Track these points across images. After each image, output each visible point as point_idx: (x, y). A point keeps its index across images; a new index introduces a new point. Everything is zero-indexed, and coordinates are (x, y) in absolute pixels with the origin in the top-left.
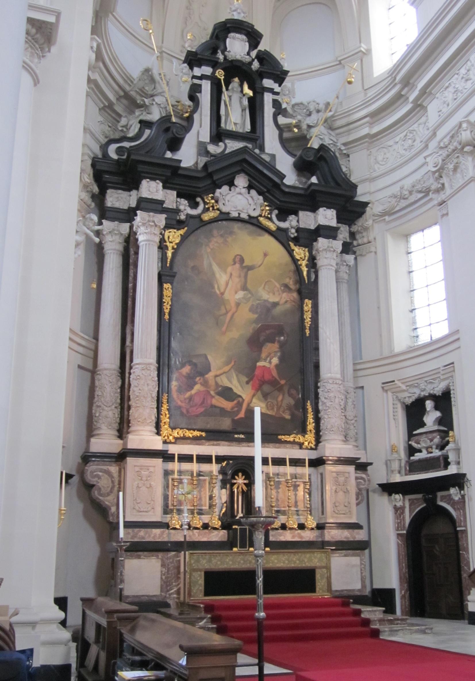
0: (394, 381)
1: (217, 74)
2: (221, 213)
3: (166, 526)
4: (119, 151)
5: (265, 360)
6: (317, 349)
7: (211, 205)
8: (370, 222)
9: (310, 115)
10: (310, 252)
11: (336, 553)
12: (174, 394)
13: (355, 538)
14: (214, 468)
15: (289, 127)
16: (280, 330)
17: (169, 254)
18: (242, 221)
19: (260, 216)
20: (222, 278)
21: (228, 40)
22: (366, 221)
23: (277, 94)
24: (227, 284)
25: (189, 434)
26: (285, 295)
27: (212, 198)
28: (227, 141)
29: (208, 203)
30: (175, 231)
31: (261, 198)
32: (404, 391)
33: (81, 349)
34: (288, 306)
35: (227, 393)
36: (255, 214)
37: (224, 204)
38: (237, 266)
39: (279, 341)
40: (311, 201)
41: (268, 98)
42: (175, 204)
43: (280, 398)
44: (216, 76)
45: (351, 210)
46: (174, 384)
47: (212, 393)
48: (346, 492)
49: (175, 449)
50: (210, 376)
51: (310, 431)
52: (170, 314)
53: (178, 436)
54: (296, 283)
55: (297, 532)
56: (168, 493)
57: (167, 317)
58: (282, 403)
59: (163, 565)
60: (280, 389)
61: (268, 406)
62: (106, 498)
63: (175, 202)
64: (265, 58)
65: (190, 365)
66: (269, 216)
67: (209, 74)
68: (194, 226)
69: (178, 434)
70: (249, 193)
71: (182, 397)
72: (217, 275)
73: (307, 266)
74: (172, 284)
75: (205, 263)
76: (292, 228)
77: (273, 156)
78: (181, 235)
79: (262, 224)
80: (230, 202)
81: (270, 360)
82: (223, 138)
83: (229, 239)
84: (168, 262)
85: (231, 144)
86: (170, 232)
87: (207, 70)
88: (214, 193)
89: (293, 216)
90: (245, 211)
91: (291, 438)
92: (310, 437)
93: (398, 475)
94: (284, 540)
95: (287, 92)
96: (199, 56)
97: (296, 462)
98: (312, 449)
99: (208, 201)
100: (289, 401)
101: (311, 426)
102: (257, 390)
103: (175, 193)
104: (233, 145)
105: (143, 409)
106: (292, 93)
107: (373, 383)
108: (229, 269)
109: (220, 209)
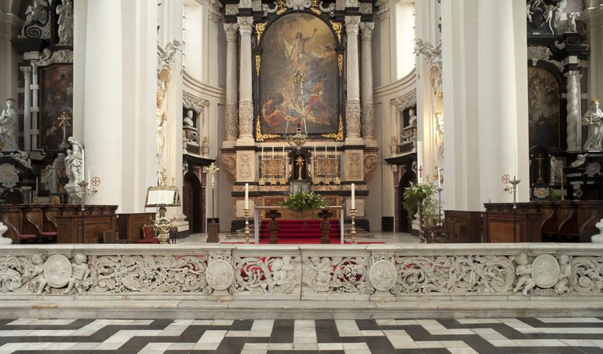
2: (288, 9)
3: (257, 184)
5: (315, 93)
12: (264, 115)
14: (284, 154)
17: (259, 38)
18: (301, 11)
19: (311, 7)
20: (289, 48)
25: (271, 136)
33: (219, 96)
34: (330, 59)
35: (293, 113)
36: (307, 6)
46: (264, 110)
49: (263, 145)
50: (283, 104)
54: (334, 45)
57: (258, 74)
60: (324, 109)
68: (272, 20)
72: (287, 47)
73: (341, 34)
74: (261, 55)
83: (293, 24)
91: (329, 136)
92: (341, 135)
98: (341, 141)
101: (341, 129)
102: (310, 110)
105: (246, 125)
107: (385, 100)
108: (294, 42)
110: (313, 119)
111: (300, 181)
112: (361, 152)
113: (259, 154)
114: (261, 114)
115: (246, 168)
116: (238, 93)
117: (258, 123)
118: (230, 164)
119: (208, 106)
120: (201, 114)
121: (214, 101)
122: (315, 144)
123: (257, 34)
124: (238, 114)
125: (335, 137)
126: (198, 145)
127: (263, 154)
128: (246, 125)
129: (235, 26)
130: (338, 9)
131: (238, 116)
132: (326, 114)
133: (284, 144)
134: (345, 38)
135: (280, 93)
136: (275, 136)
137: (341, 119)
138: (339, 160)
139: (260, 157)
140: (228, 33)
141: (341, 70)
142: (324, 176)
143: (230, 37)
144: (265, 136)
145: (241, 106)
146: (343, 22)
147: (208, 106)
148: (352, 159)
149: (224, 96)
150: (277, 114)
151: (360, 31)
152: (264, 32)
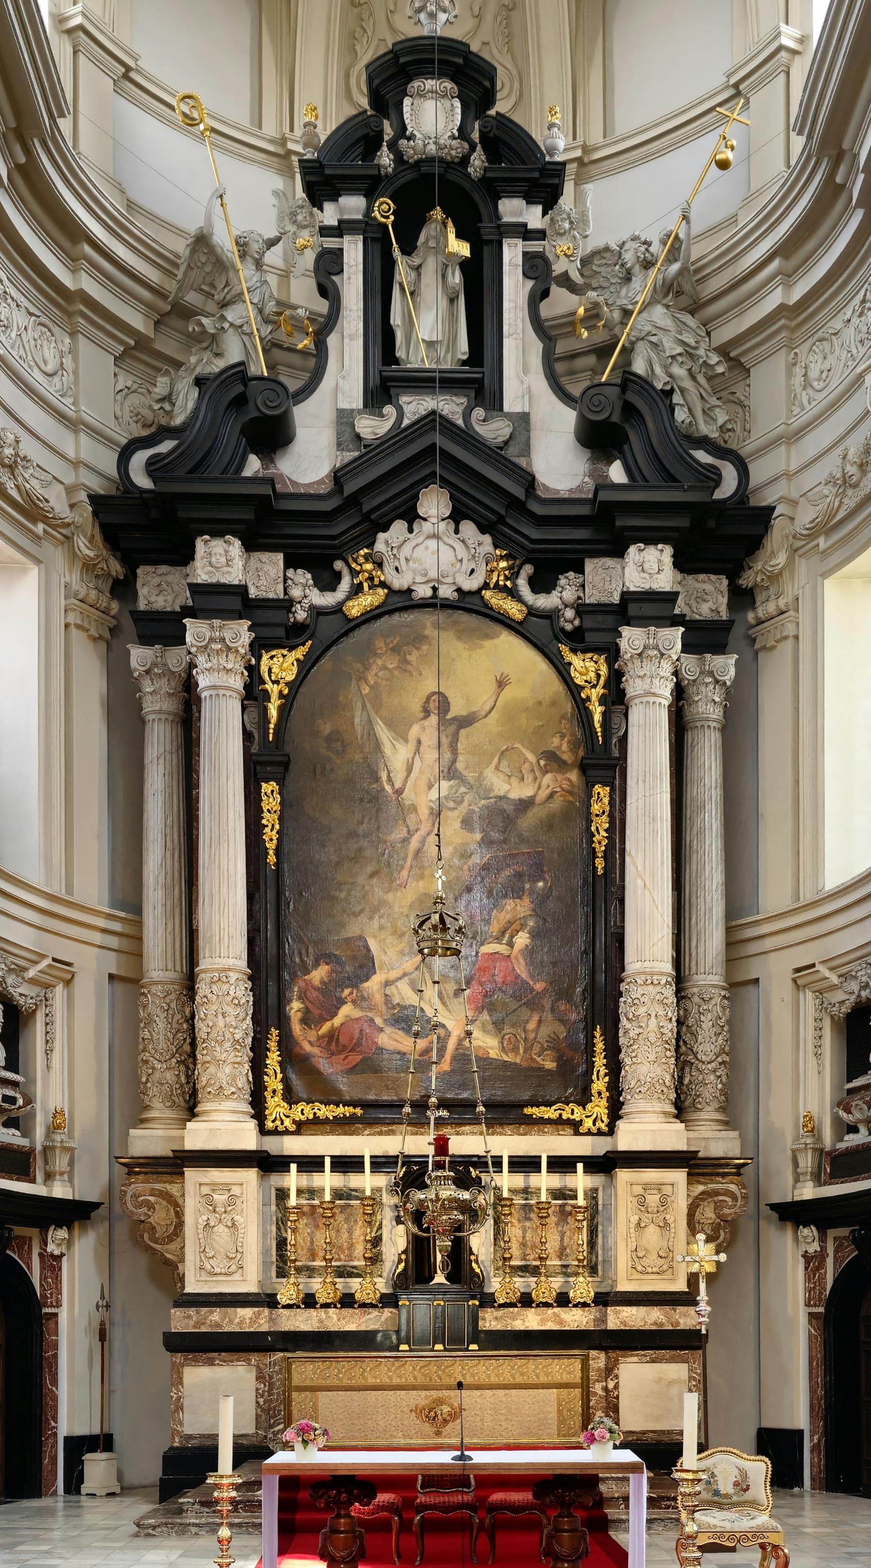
0: (813, 965)
1: (377, 214)
2: (392, 592)
5: (498, 939)
6: (622, 901)
7: (366, 575)
8: (781, 559)
9: (628, 278)
10: (610, 663)
11: (632, 1356)
13: (678, 1324)
15: (569, 324)
18: (446, 605)
19: (486, 586)
21: (407, 101)
22: (773, 554)
23: (541, 235)
24: (409, 770)
25: (325, 1112)
26: (548, 779)
27: (367, 558)
28: (404, 399)
29: (359, 573)
30: (285, 652)
31: (487, 539)
32: (833, 988)
34: (557, 804)
36: (471, 584)
37: (397, 569)
38: (433, 719)
39: (532, 892)
41: (512, 253)
42: (280, 588)
43: (532, 1026)
44: (375, 218)
45: (724, 535)
47: (379, 1021)
48: (665, 1226)
49: (294, 1145)
50: (373, 985)
51: (600, 1093)
52: (278, 852)
53: (303, 1118)
54: (574, 746)
55: (550, 1311)
56: (284, 1235)
57: (272, 858)
58: (537, 1033)
59: (260, 1378)
60: (533, 1003)
61: (505, 1043)
62: (166, 1247)
63: (281, 580)
65: (327, 964)
66: (508, 583)
67: (360, 217)
68: (325, 637)
69: (303, 1114)
70: (457, 531)
71: (312, 1035)
72: (387, 749)
74: (281, 783)
75: (357, 720)
76: (566, 606)
77: (523, 420)
78: (298, 660)
79: (491, 609)
80: (411, 563)
82: (393, 391)
83: (413, 658)
84: (271, 731)
85: (414, 403)
86: (272, 657)
87: (353, 205)
88: (371, 545)
89: (571, 574)
90: (449, 580)
91: (551, 1113)
92: (599, 1107)
93: (810, 1184)
94: (522, 1328)
95: (567, 225)
96: (328, 172)
97: (562, 1164)
98: (600, 1133)
99: (358, 568)
101: (599, 1085)
102: (480, 1009)
103: (280, 557)
105: (225, 1065)
106: (579, 222)
108: (414, 731)
109: (388, 583)
110: (487, 1043)
111: (440, 1290)
112: (679, 1176)
113: (276, 1180)
114: (283, 1023)
115: (226, 1238)
116: (192, 934)
117: (273, 1059)
118: (160, 1217)
119: (68, 983)
120: (40, 1017)
121: (92, 963)
122: (507, 1144)
123: (266, 696)
125: (576, 1117)
126: (24, 1142)
127: (293, 1179)
128: (225, 1065)
129: (175, 658)
130: (592, 597)
131: (192, 1027)
133: (366, 1144)
134: (616, 720)
135: (361, 938)
136: (341, 1110)
137: (600, 1046)
138: (593, 1210)
139: (282, 1194)
140: (148, 687)
141: (600, 849)
142: (535, 1271)
144: (303, 1111)
145: (202, 989)
146: (612, 653)
147: (68, 983)
148: (642, 1202)
150: (349, 1021)
152: (295, 686)
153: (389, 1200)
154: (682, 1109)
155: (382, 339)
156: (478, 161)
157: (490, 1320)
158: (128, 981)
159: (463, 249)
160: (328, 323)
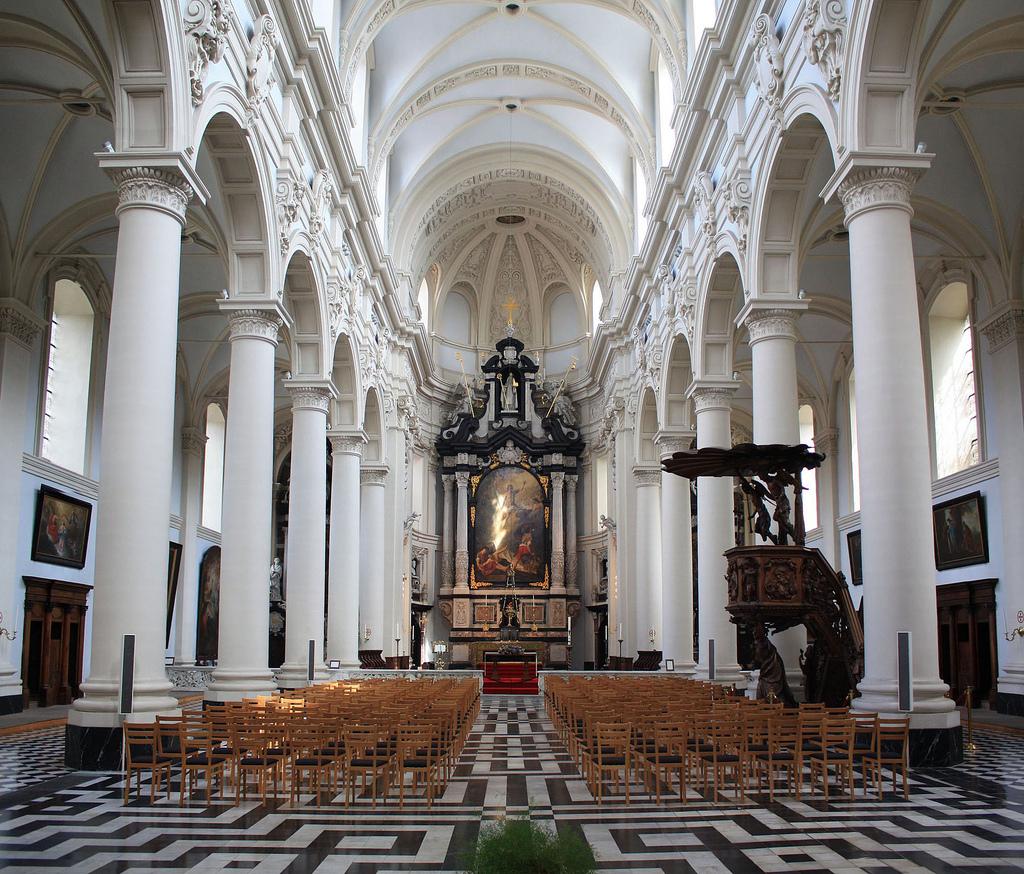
4: (448, 435)
16: (533, 525)
23: (534, 380)
25: (484, 584)
40: (549, 449)
41: (527, 385)
49: (477, 592)
64: (525, 360)
68: (486, 473)
81: (526, 543)
91: (535, 585)
100: (536, 564)
101: (546, 578)
104: (508, 422)
107: (588, 549)
110: (520, 567)
112: (564, 600)
117: (473, 571)
124: (454, 562)
132: (534, 563)
142: (532, 623)
143: (447, 487)
149: (441, 543)
151: (565, 483)
153: (499, 605)
154: (565, 585)
155: (499, 406)
156: (520, 365)
157: (521, 635)
158: (440, 552)
159: (517, 385)
160: (487, 400)
